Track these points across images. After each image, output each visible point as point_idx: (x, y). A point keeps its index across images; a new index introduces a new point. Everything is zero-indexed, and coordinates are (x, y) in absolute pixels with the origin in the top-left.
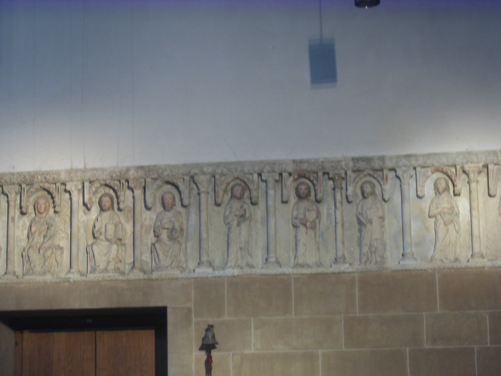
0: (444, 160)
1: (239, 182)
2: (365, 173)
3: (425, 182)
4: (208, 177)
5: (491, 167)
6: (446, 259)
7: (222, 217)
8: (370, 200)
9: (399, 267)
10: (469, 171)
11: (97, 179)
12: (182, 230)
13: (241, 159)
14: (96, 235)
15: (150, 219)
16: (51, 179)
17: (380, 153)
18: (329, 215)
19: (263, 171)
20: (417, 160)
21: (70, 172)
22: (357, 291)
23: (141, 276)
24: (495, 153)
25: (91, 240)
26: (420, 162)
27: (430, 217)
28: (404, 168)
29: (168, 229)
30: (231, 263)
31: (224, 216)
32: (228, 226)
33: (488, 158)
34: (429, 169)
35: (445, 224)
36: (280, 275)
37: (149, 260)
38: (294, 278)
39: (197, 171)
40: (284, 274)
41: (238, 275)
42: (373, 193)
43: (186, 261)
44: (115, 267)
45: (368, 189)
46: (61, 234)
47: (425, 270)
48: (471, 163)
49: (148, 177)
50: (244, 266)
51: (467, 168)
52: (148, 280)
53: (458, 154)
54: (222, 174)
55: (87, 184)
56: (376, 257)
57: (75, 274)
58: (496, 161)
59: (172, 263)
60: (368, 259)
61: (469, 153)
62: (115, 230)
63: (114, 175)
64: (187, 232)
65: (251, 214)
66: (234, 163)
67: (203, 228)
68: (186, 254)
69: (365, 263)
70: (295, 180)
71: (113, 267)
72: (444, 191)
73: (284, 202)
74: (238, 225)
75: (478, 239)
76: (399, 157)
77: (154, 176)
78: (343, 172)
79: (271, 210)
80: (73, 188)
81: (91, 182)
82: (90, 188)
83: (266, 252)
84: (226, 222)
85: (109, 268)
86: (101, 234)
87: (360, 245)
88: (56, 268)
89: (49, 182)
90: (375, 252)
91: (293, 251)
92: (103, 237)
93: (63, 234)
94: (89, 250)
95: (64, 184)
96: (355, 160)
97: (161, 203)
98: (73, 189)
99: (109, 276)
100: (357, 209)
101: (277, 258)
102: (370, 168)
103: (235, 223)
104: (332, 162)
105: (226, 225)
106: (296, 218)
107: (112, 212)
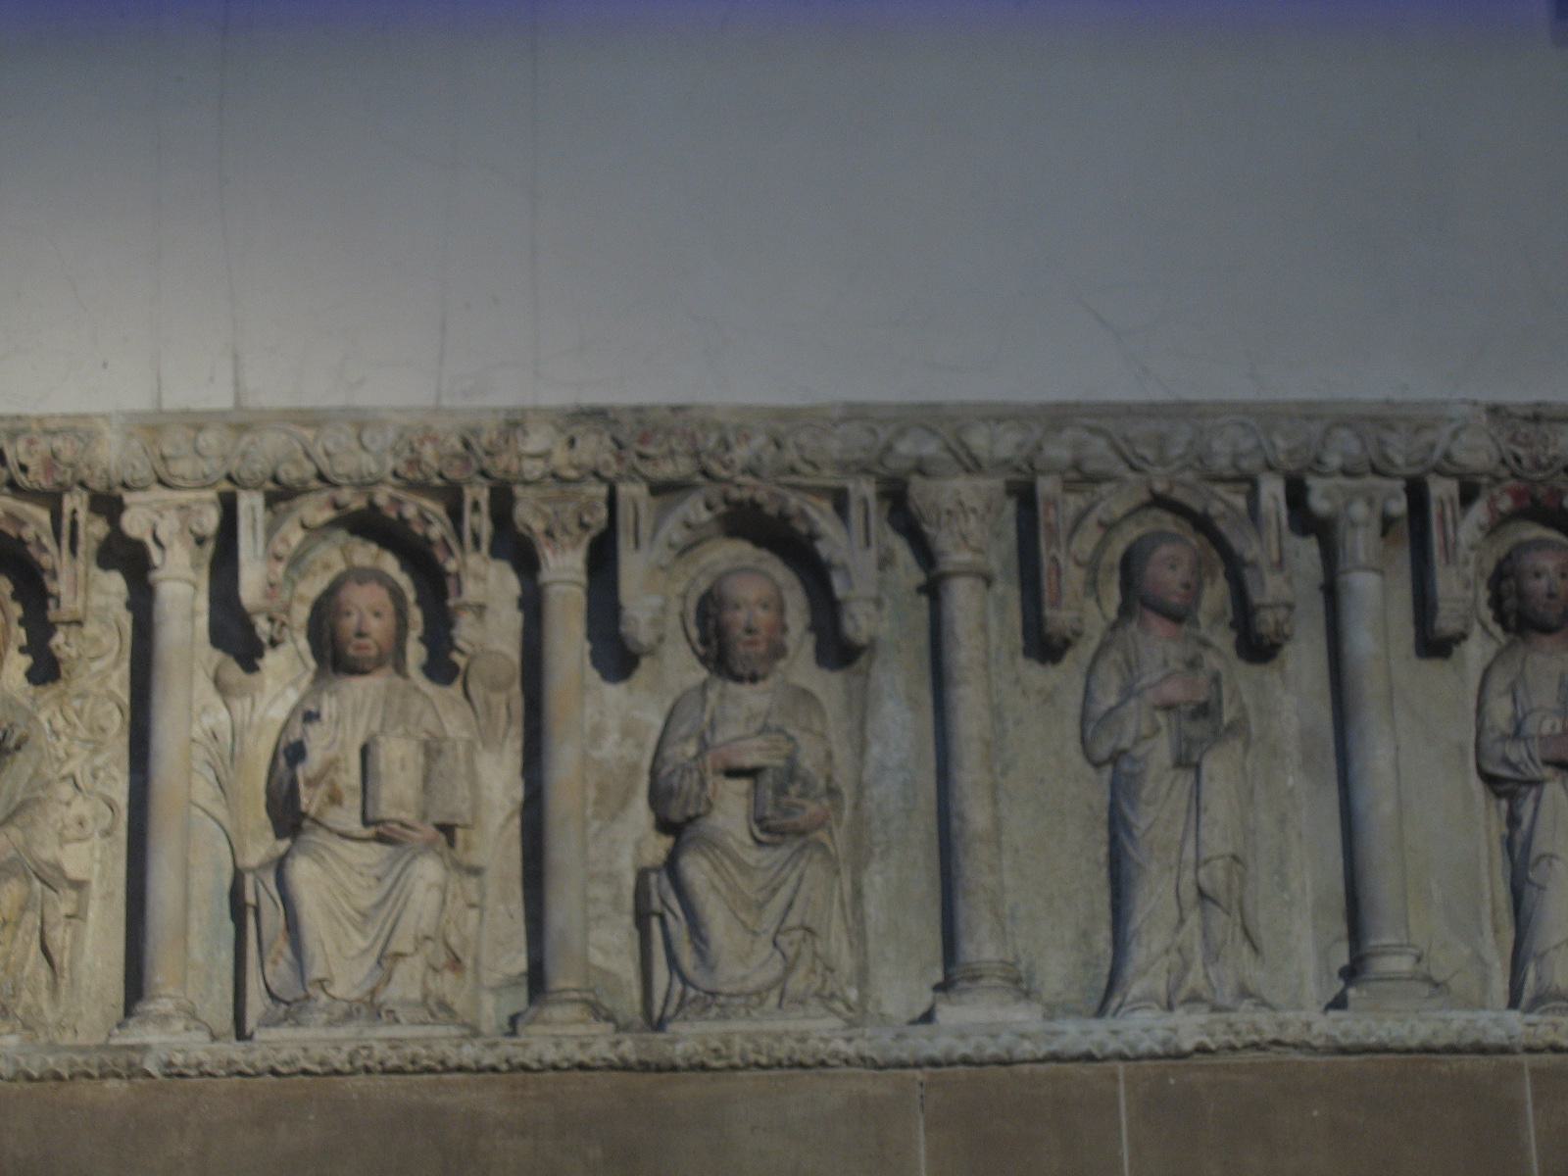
1: (1168, 521)
4: (997, 483)
7: (1072, 728)
11: (321, 477)
12: (832, 792)
13: (1192, 396)
14: (310, 800)
15: (628, 731)
16: (33, 464)
19: (1317, 466)
21: (151, 426)
23: (601, 1044)
25: (261, 847)
29: (752, 773)
30: (1147, 975)
31: (1084, 718)
32: (1108, 770)
36: (1452, 1049)
37: (627, 969)
38: (1533, 1071)
39: (931, 448)
40: (1480, 1049)
41: (1202, 1049)
43: (862, 977)
44: (425, 997)
46: (68, 804)
49: (634, 475)
50: (1228, 1001)
52: (645, 1067)
54: (1082, 478)
55: (250, 504)
57: (179, 1025)
59: (789, 968)
62: (426, 780)
63: (428, 452)
64: (856, 807)
65: (1242, 708)
66: (1152, 410)
67: (970, 774)
68: (858, 935)
70: (1498, 524)
71: (415, 994)
73: (1434, 645)
74: (1186, 762)
77: (667, 470)
79: (1369, 684)
80: (169, 527)
81: (280, 495)
82: (271, 530)
83: (1341, 928)
84: (1103, 750)
85: (392, 993)
86: (335, 798)
88: (45, 995)
89: (21, 478)
91: (1496, 931)
92: (348, 818)
93: (81, 807)
94: (261, 892)
95: (109, 505)
97: (694, 633)
98: (163, 535)
99: (395, 1044)
101: (1419, 959)
103: (1161, 751)
105: (1097, 765)
106: (1517, 733)
107: (398, 680)
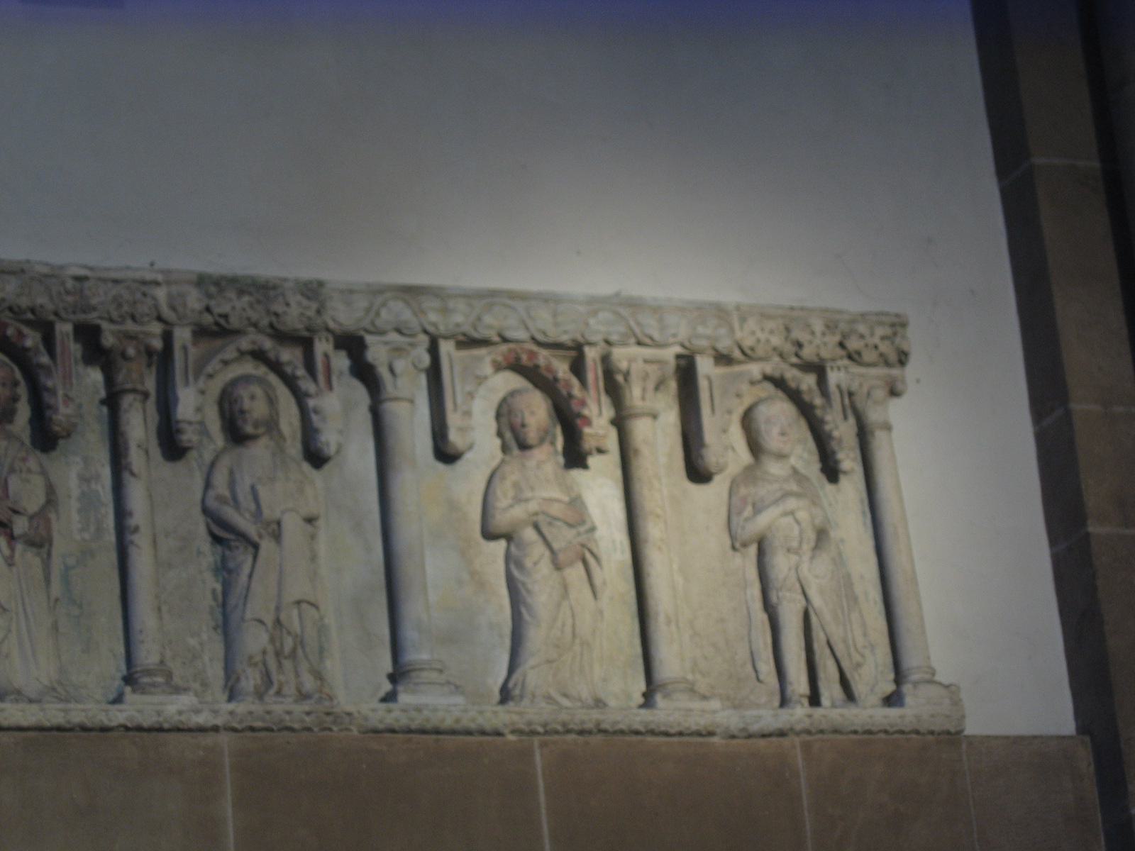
0: (546, 323)
2: (245, 344)
3: (471, 395)
5: (705, 366)
6: (565, 695)
8: (260, 451)
9: (393, 716)
10: (627, 375)
17: (307, 273)
18: (88, 502)
20: (445, 311)
22: (227, 807)
24: (720, 312)
26: (460, 318)
27: (489, 534)
28: (394, 337)
33: (701, 330)
34: (481, 351)
35: (558, 566)
42: (271, 425)
45: (256, 408)
47: (498, 734)
48: (639, 343)
51: (623, 356)
53: (595, 303)
56: (297, 675)
58: (724, 345)
60: (267, 677)
61: (635, 305)
69: (260, 695)
72: (542, 441)
75: (673, 628)
76: (377, 291)
78: (157, 328)
87: (227, 627)
90: (293, 655)
96: (211, 284)
100: (208, 485)
102: (264, 322)
104: (116, 281)
